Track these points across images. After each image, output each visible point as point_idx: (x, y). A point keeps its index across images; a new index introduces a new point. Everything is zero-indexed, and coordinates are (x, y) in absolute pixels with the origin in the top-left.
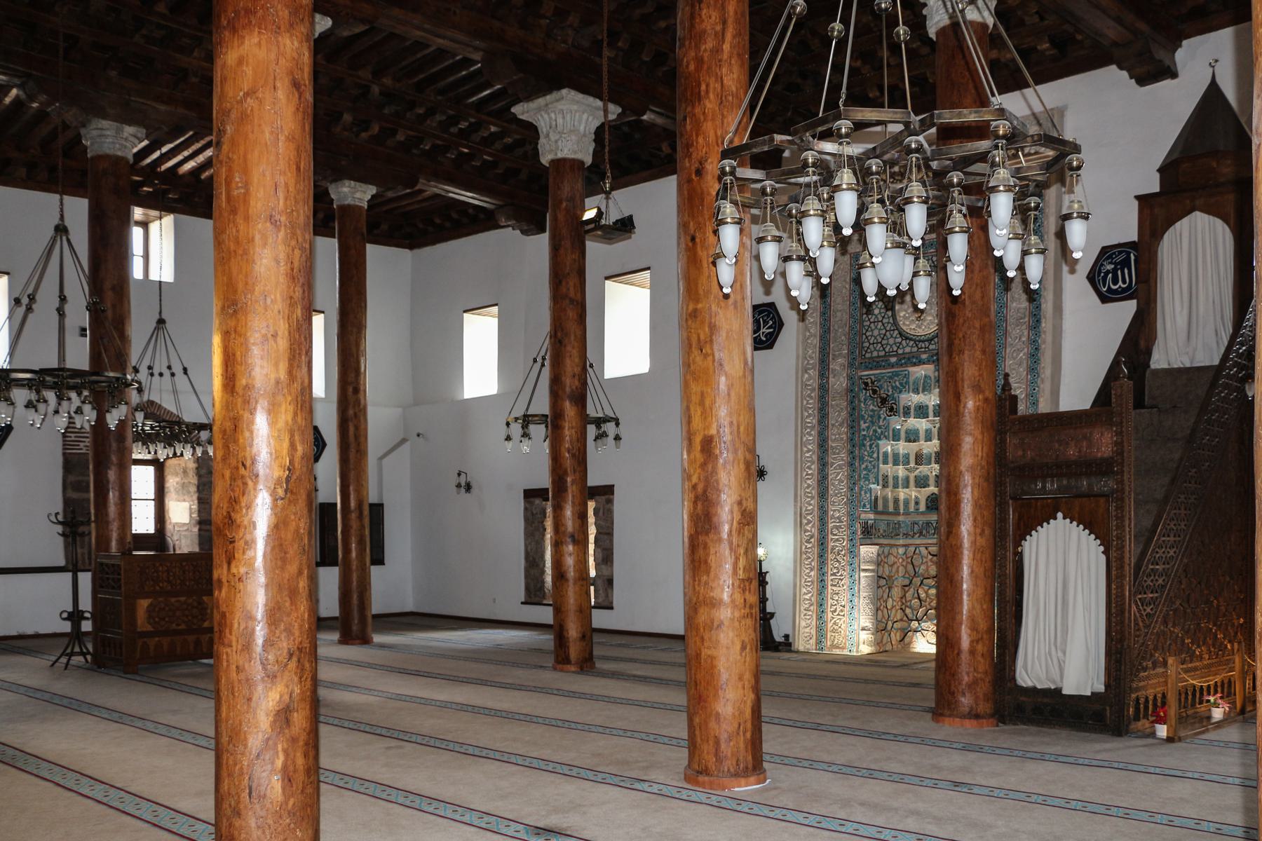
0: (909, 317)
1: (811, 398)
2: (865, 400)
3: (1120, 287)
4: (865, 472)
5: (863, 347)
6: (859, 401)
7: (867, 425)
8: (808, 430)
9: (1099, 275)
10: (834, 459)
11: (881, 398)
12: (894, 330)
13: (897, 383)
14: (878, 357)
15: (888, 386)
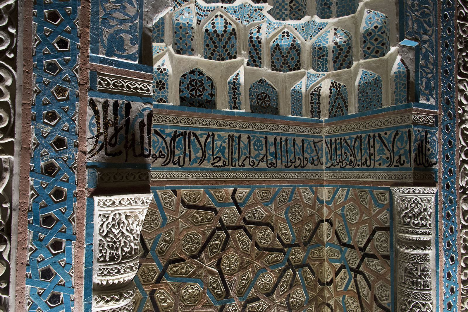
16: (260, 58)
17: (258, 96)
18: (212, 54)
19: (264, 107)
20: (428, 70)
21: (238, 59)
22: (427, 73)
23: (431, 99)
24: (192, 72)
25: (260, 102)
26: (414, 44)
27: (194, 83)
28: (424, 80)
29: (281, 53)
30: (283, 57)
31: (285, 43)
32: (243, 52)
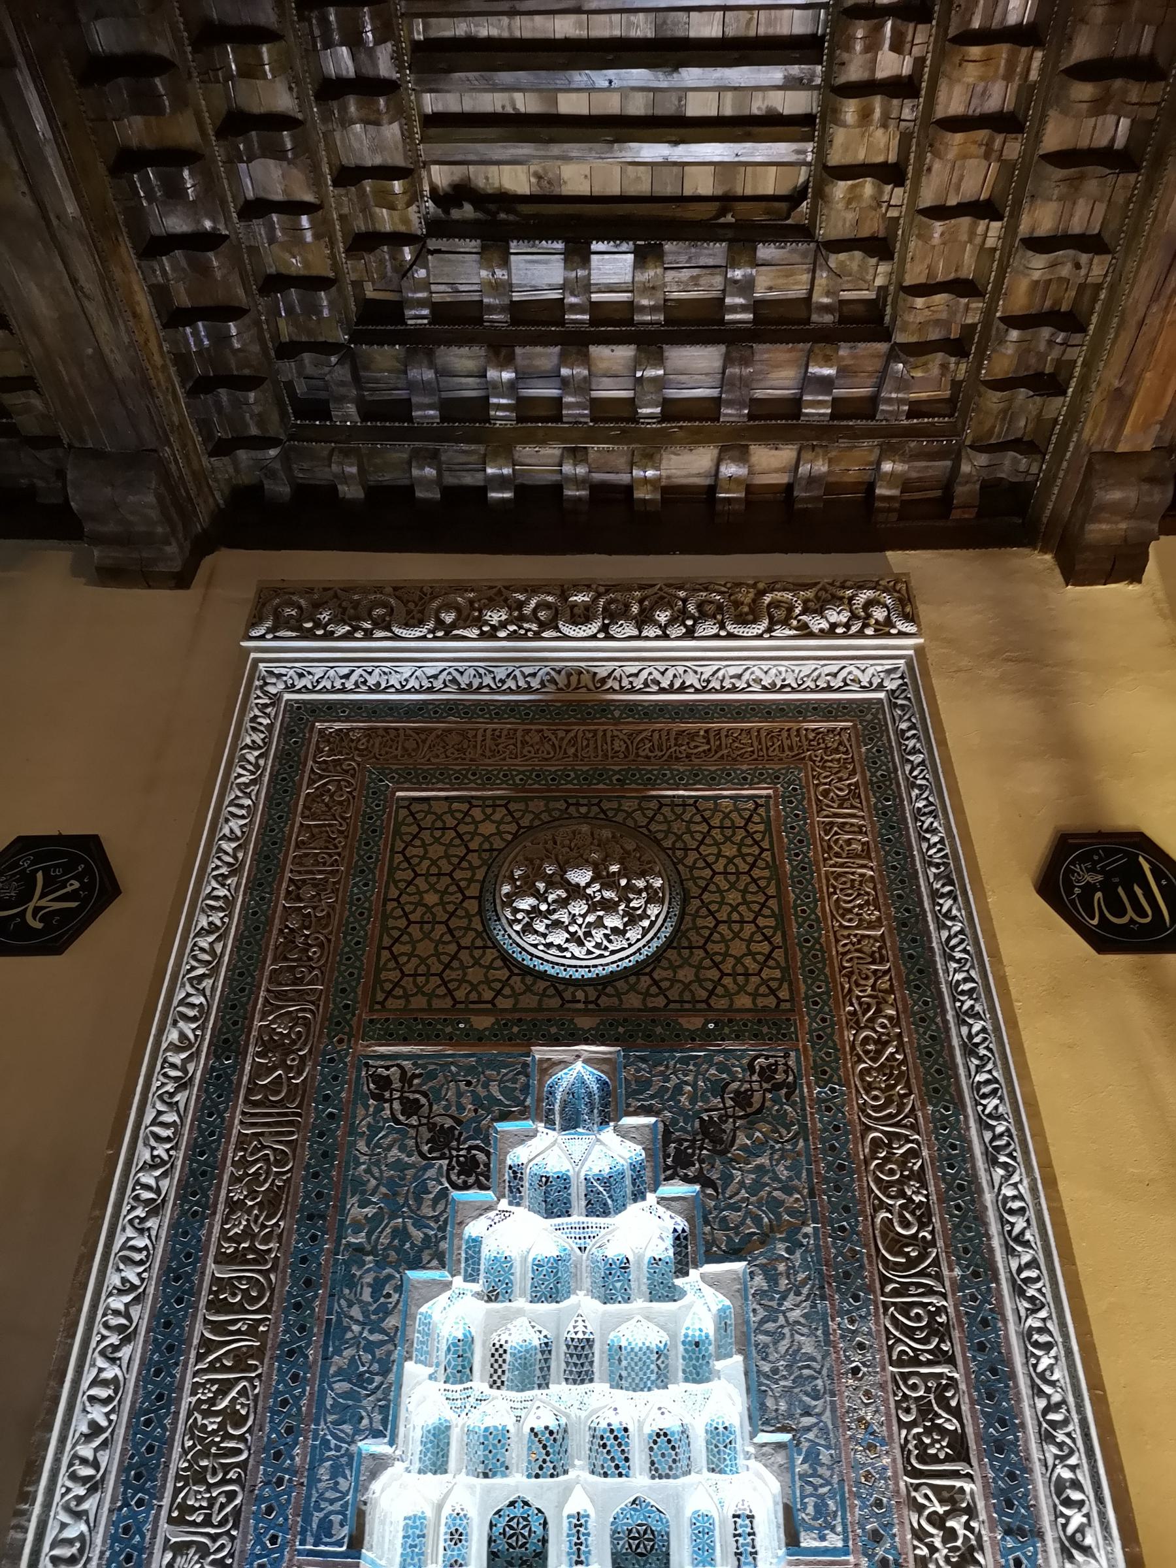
0: (550, 911)
1: (173, 1106)
2: (374, 1130)
3: (1132, 921)
4: (342, 1386)
5: (378, 981)
6: (352, 1130)
7: (369, 1211)
8: (140, 1212)
9: (1070, 892)
10: (218, 1328)
11: (432, 1127)
12: (485, 947)
13: (495, 1090)
14: (430, 1009)
15: (460, 1094)
16: (627, 1460)
17: (630, 1531)
18: (541, 1468)
19: (641, 1555)
20: (817, 1481)
21: (572, 1474)
22: (816, 1488)
23: (831, 1536)
24: (512, 1504)
25: (634, 1543)
26: (785, 1437)
27: (513, 1524)
28: (810, 1501)
29: (669, 1441)
30: (673, 1448)
31: (670, 1423)
32: (577, 1462)
